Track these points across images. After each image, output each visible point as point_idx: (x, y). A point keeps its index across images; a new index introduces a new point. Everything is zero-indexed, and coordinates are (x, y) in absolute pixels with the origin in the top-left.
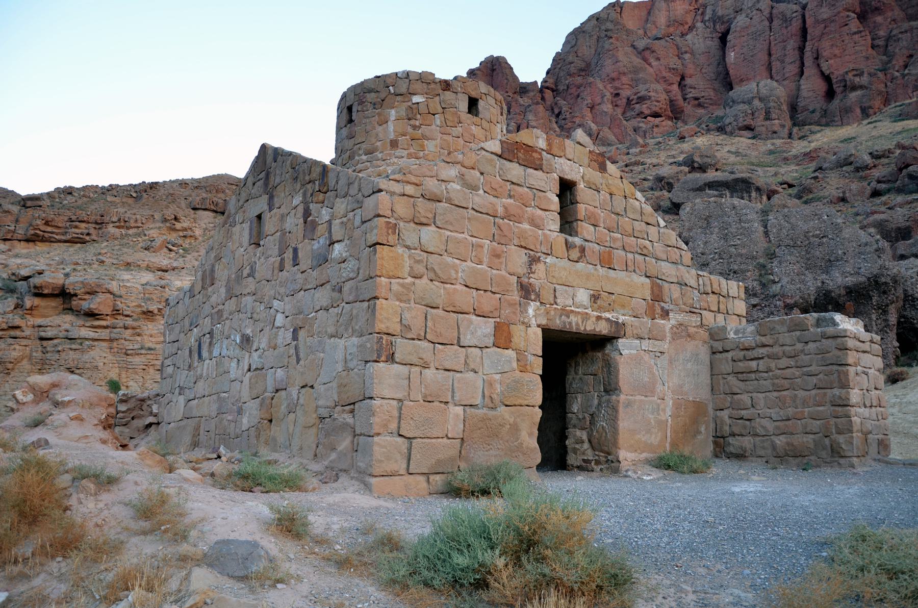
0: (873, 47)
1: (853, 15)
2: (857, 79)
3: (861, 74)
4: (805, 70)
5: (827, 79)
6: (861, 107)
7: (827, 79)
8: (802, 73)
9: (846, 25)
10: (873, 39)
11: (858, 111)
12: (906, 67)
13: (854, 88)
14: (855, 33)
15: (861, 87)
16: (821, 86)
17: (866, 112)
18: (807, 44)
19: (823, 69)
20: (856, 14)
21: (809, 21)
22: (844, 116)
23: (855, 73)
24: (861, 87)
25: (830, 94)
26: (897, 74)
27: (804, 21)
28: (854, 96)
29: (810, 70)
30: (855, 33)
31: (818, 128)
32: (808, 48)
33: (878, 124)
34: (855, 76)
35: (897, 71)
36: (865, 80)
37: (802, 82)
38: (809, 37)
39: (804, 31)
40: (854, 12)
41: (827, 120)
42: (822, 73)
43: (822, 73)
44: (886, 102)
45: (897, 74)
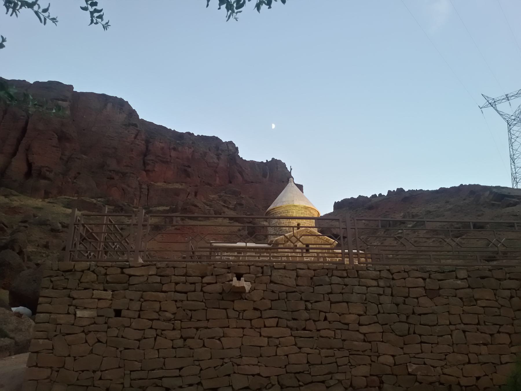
0: (61, 159)
1: (56, 136)
2: (48, 173)
3: (50, 171)
4: (17, 154)
5: (30, 165)
6: (45, 191)
7: (30, 165)
8: (14, 154)
9: (51, 139)
10: (62, 155)
11: (43, 192)
12: (75, 178)
13: (45, 178)
14: (54, 146)
15: (49, 179)
16: (24, 168)
17: (47, 195)
18: (24, 138)
19: (29, 158)
20: (58, 136)
21: (30, 126)
22: (34, 192)
23: (47, 169)
24: (49, 179)
25: (28, 174)
26: (70, 180)
27: (27, 124)
28: (43, 182)
29: (21, 155)
30: (54, 146)
31: (16, 193)
32: (24, 142)
33: (55, 205)
34: (47, 171)
35: (70, 179)
36: (51, 175)
37: (13, 160)
38: (26, 135)
39: (24, 131)
40: (57, 134)
41: (22, 190)
42: (27, 160)
43: (27, 160)
44: (60, 193)
45: (70, 180)
